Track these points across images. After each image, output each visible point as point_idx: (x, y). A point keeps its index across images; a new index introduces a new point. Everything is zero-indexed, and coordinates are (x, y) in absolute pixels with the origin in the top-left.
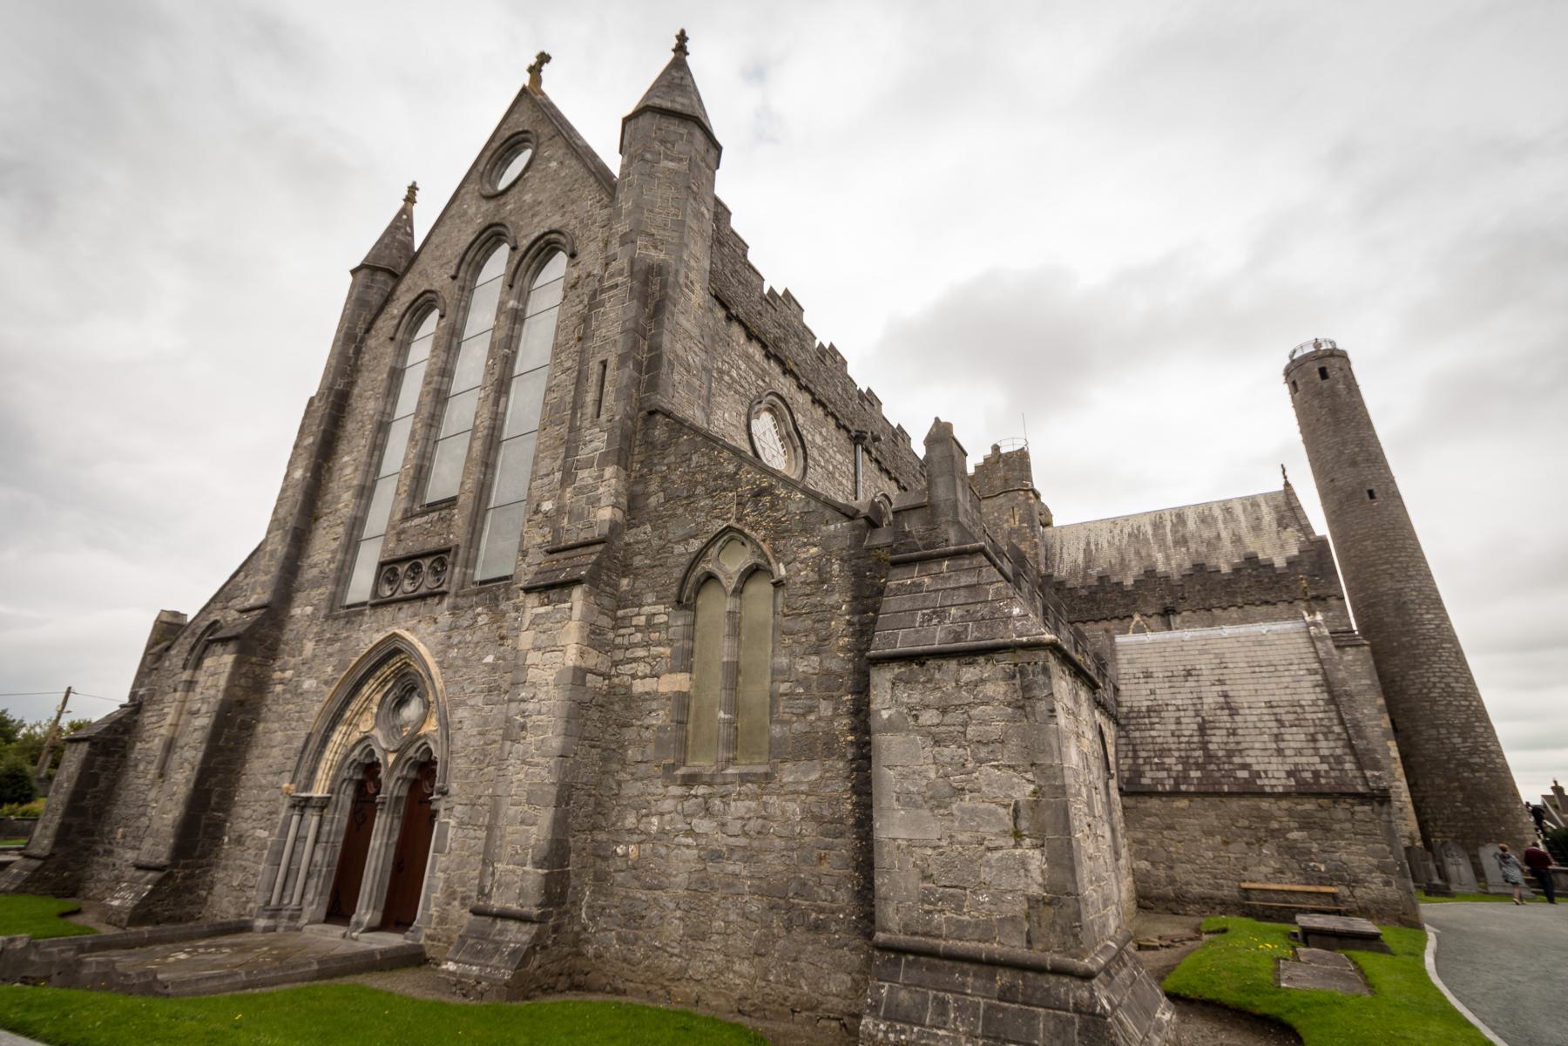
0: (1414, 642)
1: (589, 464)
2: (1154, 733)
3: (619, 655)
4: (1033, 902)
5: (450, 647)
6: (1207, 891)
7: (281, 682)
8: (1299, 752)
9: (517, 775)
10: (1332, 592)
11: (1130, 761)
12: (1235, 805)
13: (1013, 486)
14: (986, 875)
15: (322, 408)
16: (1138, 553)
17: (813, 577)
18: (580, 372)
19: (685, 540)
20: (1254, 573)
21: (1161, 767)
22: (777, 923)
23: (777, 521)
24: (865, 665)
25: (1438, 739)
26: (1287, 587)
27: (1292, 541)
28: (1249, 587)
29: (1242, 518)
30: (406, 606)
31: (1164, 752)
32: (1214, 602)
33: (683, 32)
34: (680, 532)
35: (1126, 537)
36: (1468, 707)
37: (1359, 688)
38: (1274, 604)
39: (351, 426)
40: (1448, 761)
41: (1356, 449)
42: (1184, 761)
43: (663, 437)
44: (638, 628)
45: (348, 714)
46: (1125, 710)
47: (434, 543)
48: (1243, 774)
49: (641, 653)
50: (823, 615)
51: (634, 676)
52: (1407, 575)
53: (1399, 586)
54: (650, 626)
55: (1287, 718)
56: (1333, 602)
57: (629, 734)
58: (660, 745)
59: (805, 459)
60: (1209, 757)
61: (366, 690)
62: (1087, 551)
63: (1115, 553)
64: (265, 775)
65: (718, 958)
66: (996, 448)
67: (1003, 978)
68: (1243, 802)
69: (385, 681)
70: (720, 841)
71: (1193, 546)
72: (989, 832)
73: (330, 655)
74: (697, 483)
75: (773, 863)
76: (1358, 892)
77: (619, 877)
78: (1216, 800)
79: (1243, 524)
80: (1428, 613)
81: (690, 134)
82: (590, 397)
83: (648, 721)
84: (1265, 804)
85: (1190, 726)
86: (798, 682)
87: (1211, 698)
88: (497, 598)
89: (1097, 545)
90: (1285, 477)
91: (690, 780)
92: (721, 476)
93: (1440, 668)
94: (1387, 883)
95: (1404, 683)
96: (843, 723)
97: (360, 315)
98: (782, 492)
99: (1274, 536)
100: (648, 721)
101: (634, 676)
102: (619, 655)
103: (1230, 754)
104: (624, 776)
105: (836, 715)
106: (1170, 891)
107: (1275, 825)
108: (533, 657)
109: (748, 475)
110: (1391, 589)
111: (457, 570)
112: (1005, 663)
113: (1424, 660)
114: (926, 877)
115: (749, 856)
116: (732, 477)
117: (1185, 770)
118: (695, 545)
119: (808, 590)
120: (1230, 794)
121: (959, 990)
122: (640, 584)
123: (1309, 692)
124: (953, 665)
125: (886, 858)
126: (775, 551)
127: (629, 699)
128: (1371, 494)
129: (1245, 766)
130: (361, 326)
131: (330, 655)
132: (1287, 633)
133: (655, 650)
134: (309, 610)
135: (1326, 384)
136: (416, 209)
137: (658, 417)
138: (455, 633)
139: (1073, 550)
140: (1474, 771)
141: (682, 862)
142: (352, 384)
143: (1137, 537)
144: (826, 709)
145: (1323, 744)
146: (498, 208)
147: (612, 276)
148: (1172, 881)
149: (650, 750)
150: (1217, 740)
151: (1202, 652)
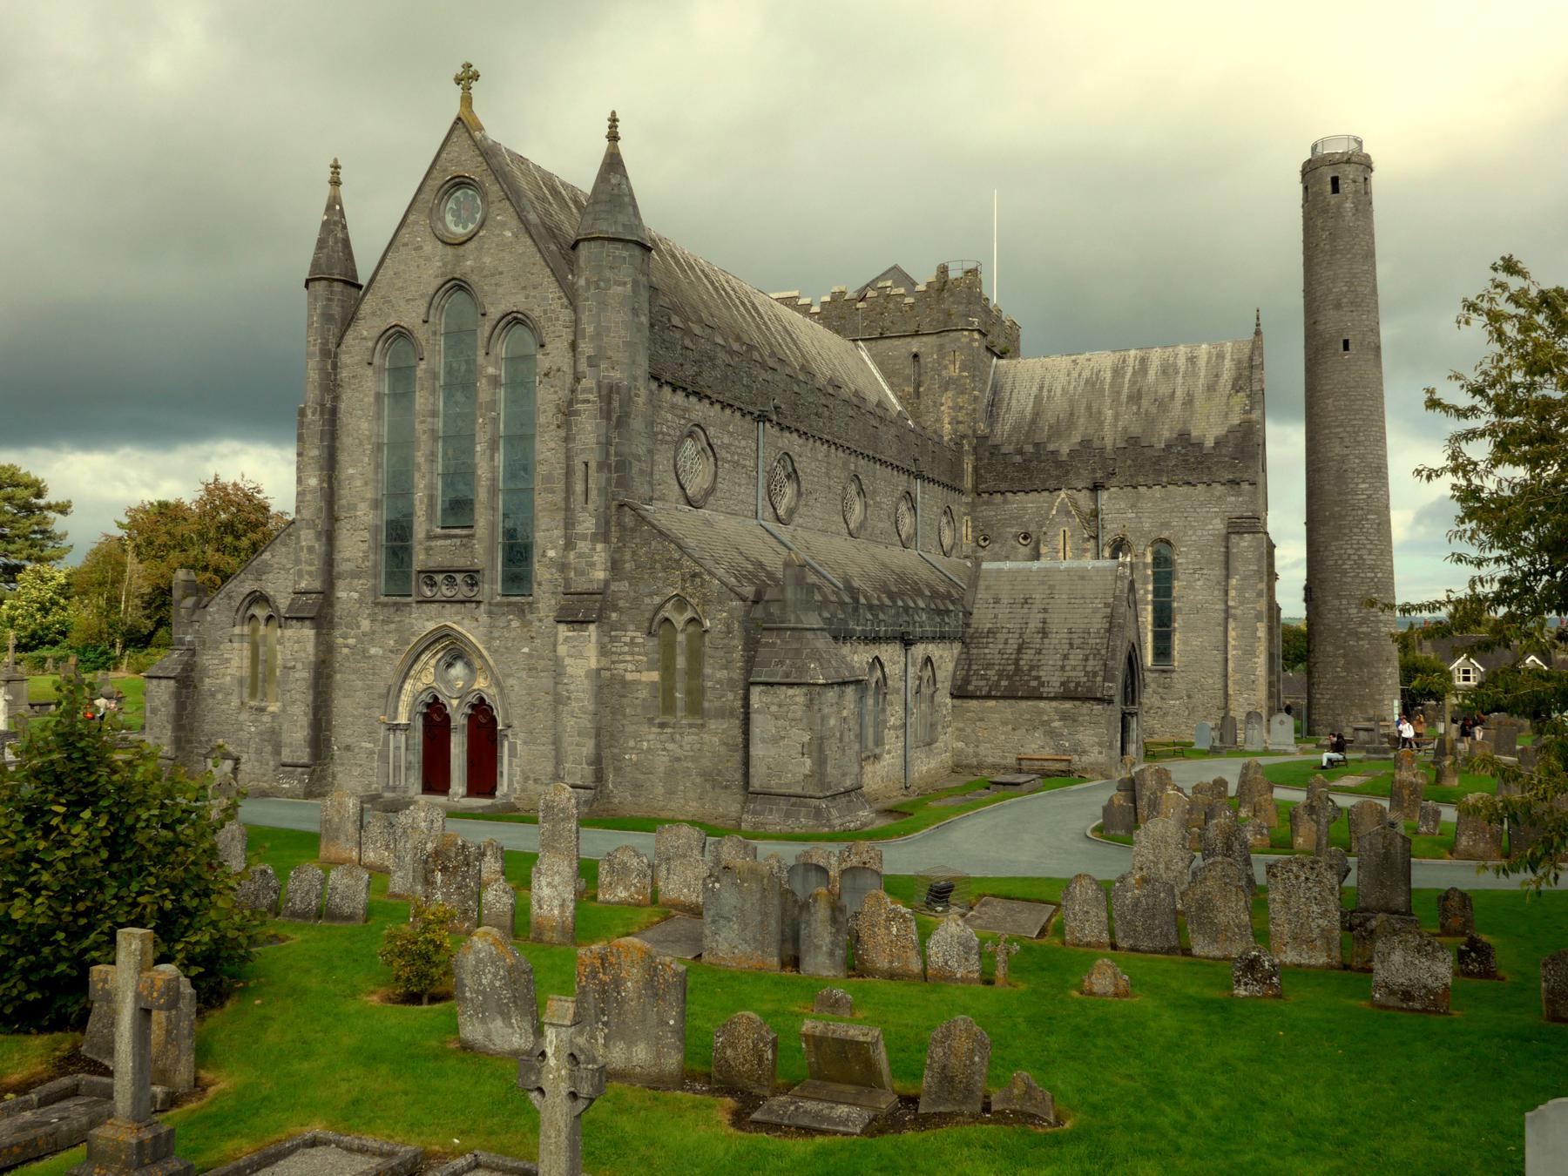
0: (1344, 513)
1: (584, 537)
2: (987, 651)
3: (615, 658)
4: (806, 776)
5: (493, 638)
6: (997, 760)
7: (346, 646)
8: (1074, 669)
9: (569, 722)
10: (1246, 476)
11: (964, 672)
12: (1024, 704)
13: (957, 325)
14: (790, 767)
16: (1089, 407)
17: (724, 629)
18: (568, 466)
19: (651, 595)
20: (1183, 451)
21: (984, 677)
22: (708, 786)
23: (705, 594)
24: (748, 686)
25: (1339, 610)
26: (1209, 468)
27: (1237, 409)
28: (1176, 465)
29: (1202, 373)
30: (448, 606)
31: (988, 666)
32: (1141, 480)
33: (614, 113)
34: (647, 590)
35: (1082, 383)
36: (1372, 579)
39: (346, 441)
40: (1341, 631)
41: (1345, 289)
42: (1000, 674)
43: (631, 524)
44: (626, 644)
45: (412, 672)
46: (972, 630)
47: (460, 563)
48: (1034, 683)
49: (629, 658)
50: (730, 650)
51: (626, 670)
52: (1355, 441)
53: (1346, 451)
54: (632, 643)
55: (1077, 642)
56: (1245, 486)
57: (625, 701)
59: (716, 459)
60: (1018, 670)
61: (424, 658)
62: (1038, 399)
63: (1065, 405)
64: (356, 709)
65: (682, 801)
66: (943, 270)
67: (793, 799)
68: (1030, 703)
69: (437, 652)
70: (679, 753)
71: (1145, 403)
72: (793, 753)
73: (388, 632)
74: (655, 561)
75: (706, 763)
76: (1083, 759)
77: (628, 769)
78: (1013, 702)
79: (1201, 381)
80: (1363, 482)
82: (579, 488)
83: (636, 695)
84: (1042, 704)
85: (1012, 648)
86: (717, 682)
87: (1034, 624)
88: (523, 611)
89: (1050, 391)
90: (1258, 325)
91: (662, 725)
92: (670, 559)
94: (1100, 753)
95: (1327, 553)
96: (739, 703)
97: (329, 330)
98: (707, 577)
99: (1224, 399)
100: (636, 695)
101: (626, 670)
102: (615, 658)
103: (1032, 668)
104: (625, 722)
105: (735, 699)
106: (974, 762)
107: (1046, 718)
108: (568, 661)
109: (686, 562)
111: (486, 586)
112: (804, 690)
113: (1347, 531)
114: (769, 768)
115: (695, 760)
116: (677, 561)
117: (999, 680)
118: (657, 600)
119: (722, 636)
120: (1022, 698)
121: (778, 804)
122: (624, 618)
123: (1098, 624)
124: (784, 688)
125: (753, 762)
126: (704, 612)
127: (624, 683)
129: (1038, 678)
130: (333, 340)
131: (388, 632)
132: (1105, 569)
133: (637, 657)
134: (355, 595)
135: (1334, 199)
136: (344, 191)
137: (626, 508)
138: (494, 630)
139: (1023, 395)
140: (1360, 639)
141: (661, 762)
142: (336, 398)
143: (1093, 385)
144: (730, 696)
145: (1091, 662)
146: (459, 259)
147: (584, 391)
148: (976, 755)
149: (639, 710)
150: (1028, 656)
151: (1042, 583)
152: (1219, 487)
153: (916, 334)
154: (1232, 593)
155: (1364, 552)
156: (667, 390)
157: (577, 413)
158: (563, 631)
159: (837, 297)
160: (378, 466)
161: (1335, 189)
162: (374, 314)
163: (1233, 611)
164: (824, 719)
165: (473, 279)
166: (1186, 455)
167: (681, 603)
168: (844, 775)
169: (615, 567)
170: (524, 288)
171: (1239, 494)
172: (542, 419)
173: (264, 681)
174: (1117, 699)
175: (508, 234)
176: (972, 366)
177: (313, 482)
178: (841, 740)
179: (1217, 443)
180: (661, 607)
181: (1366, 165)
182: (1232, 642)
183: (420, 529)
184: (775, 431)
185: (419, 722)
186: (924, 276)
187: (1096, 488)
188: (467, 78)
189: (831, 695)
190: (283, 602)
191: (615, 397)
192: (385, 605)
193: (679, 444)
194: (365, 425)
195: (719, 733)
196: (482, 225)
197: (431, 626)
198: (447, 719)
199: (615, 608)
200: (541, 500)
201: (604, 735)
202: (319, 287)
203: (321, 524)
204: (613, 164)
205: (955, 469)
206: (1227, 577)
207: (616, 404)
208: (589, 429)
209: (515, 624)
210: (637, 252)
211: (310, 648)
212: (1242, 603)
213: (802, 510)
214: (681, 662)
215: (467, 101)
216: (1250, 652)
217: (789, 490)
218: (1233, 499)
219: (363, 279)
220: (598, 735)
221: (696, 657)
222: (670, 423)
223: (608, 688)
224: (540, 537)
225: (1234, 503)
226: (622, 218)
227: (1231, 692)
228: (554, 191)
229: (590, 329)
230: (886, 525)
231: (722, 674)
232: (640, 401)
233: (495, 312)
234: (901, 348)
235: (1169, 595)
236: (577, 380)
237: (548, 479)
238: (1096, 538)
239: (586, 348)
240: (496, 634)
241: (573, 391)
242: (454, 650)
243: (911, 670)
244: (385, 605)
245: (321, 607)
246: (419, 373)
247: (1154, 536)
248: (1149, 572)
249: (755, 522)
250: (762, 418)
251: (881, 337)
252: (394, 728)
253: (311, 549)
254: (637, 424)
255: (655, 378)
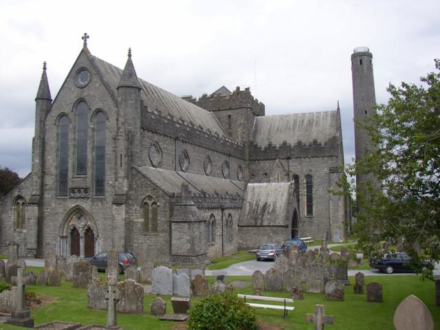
1: (121, 178)
15: (38, 142)
24: (171, 222)
39: (47, 148)
47: (82, 186)
58: (140, 230)
66: (238, 88)
70: (151, 244)
81: (135, 92)
91: (145, 235)
108: (116, 216)
115: (155, 246)
118: (143, 197)
122: (133, 202)
125: (173, 245)
128: (366, 112)
141: (145, 246)
144: (166, 226)
146: (82, 92)
153: (230, 109)
156: (146, 131)
157: (118, 139)
158: (114, 207)
159: (205, 96)
160: (57, 156)
161: (361, 63)
162: (56, 109)
164: (194, 232)
165: (86, 98)
167: (150, 197)
168: (201, 249)
169: (130, 187)
170: (102, 101)
171: (332, 160)
172: (108, 141)
173: (22, 223)
174: (290, 226)
175: (97, 84)
176: (247, 119)
177: (37, 161)
178: (200, 238)
179: (325, 144)
180: (145, 199)
181: (370, 56)
182: (331, 208)
183: (70, 174)
184: (181, 143)
185: (69, 235)
186: (232, 89)
187: (289, 158)
188: (85, 37)
189: (196, 225)
190: (28, 198)
191: (130, 134)
192: (59, 199)
193: (150, 148)
194: (53, 143)
195: (162, 237)
196: (89, 82)
197: (74, 205)
198: (79, 234)
199: (130, 199)
200: (107, 166)
201: (128, 240)
202: (40, 101)
203: (40, 174)
204: (130, 64)
205: (242, 152)
207: (130, 137)
208: (122, 145)
209: (99, 204)
210: (137, 90)
211: (37, 212)
213: (191, 168)
214: (150, 216)
215: (85, 44)
216: (337, 211)
217: (186, 162)
219: (53, 98)
220: (125, 239)
221: (155, 214)
222: (147, 142)
223: (129, 224)
224: (107, 177)
225: (331, 163)
226: (132, 80)
227: (331, 223)
228: (113, 71)
229: (122, 114)
230: (219, 172)
231: (163, 219)
232: (138, 135)
233: (93, 109)
234: (225, 114)
235: (311, 193)
236: (118, 129)
237: (109, 160)
238: (288, 175)
239: (121, 119)
240: (94, 207)
241: (117, 133)
242: (79, 212)
243: (224, 218)
244: (59, 199)
245: (40, 199)
246: (70, 127)
247: (306, 174)
248: (305, 185)
249: (175, 172)
250: (177, 139)
251: (219, 110)
252: (62, 237)
253: (36, 182)
254: (137, 142)
255: (142, 128)
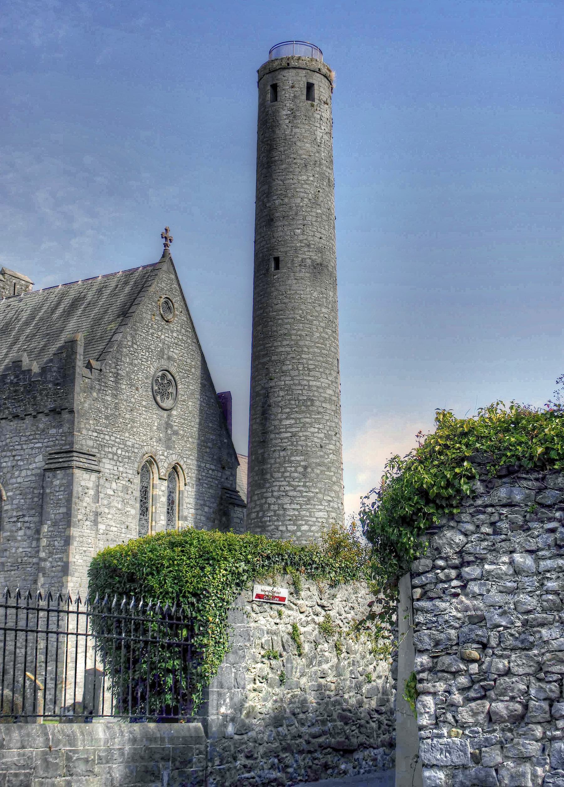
36: (294, 532)
37: (58, 517)
38: (23, 419)
56: (66, 416)
80: (287, 418)
93: (280, 486)
110: (263, 388)
152: (44, 419)
154: (44, 542)
155: (286, 500)
163: (43, 564)
166: (17, 384)
206: (41, 523)
212: (51, 554)
218: (53, 431)
